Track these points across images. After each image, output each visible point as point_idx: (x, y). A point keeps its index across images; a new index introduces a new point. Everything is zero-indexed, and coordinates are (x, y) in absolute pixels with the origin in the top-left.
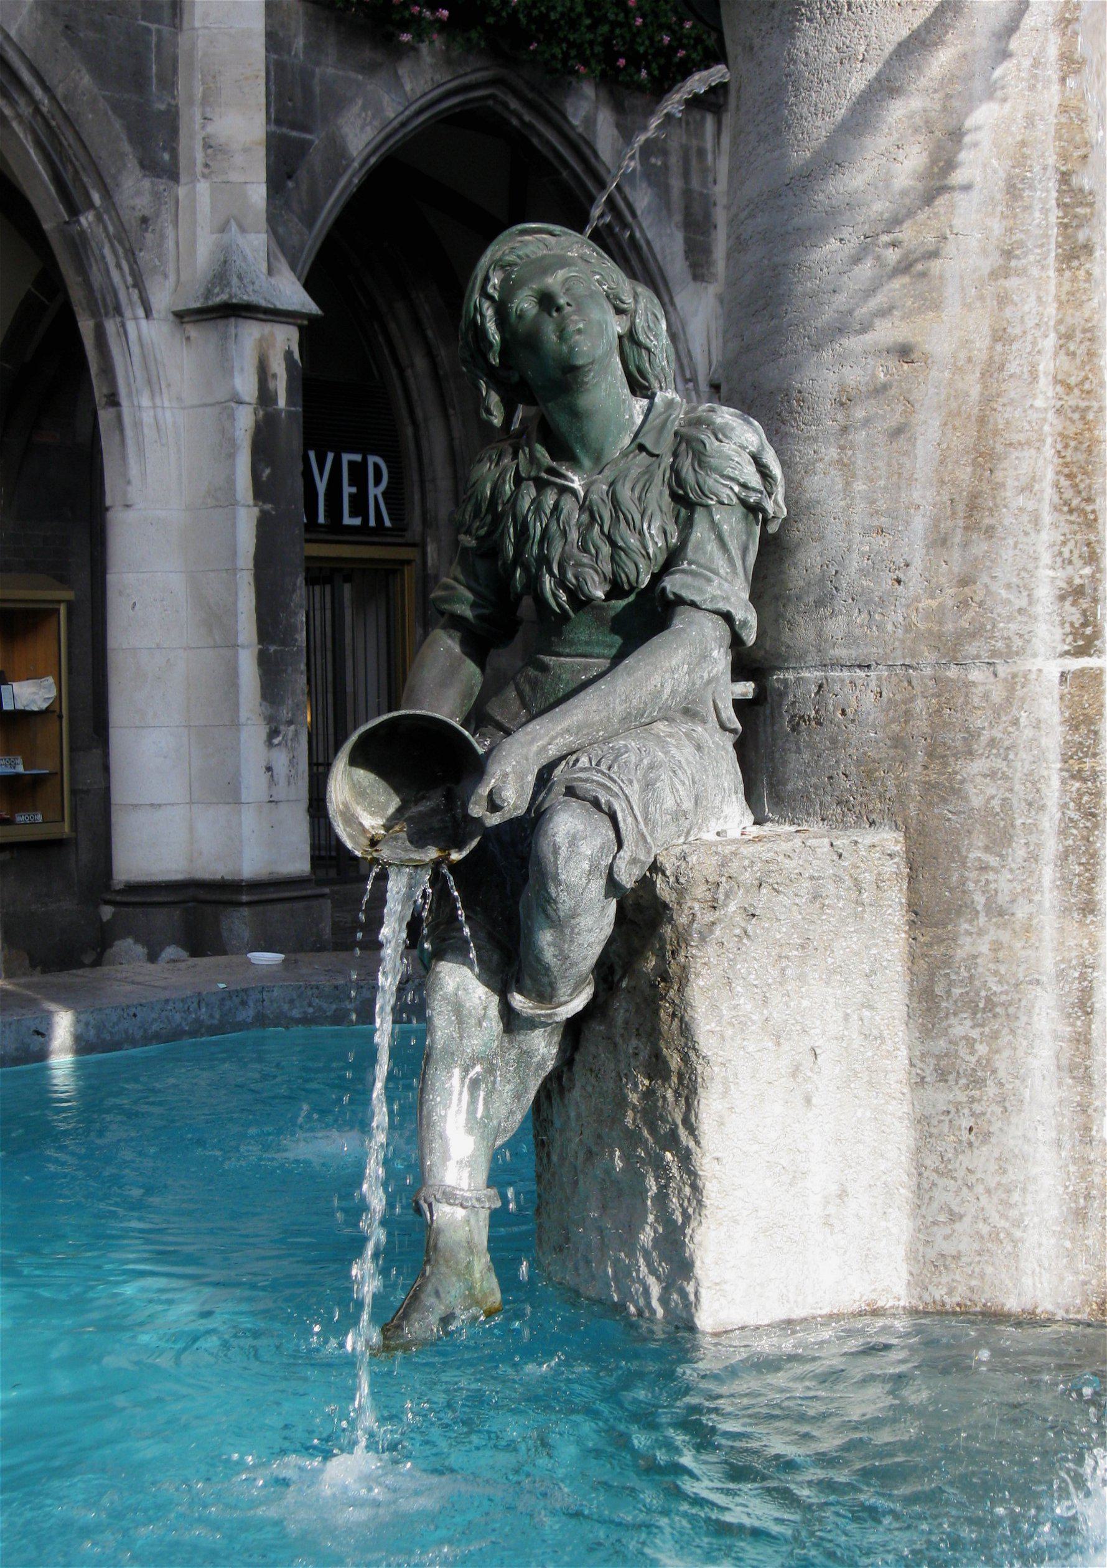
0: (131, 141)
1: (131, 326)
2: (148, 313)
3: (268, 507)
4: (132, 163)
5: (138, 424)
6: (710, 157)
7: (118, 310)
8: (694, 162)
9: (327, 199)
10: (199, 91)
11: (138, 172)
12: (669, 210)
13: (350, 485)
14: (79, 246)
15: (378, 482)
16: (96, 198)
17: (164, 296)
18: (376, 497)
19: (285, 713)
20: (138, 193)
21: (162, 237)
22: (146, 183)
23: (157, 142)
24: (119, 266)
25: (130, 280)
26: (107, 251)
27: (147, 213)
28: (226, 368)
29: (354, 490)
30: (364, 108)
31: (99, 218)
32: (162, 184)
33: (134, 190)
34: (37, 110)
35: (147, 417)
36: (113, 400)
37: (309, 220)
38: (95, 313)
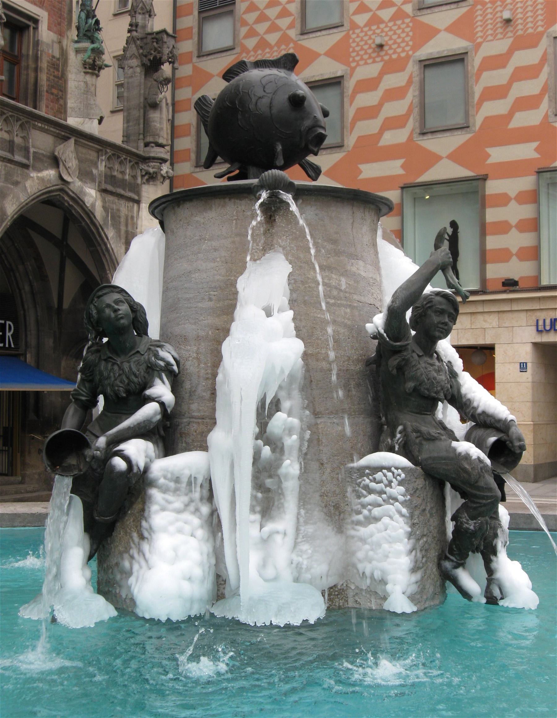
6: (135, 219)
8: (130, 221)
12: (120, 236)
30: (13, 198)
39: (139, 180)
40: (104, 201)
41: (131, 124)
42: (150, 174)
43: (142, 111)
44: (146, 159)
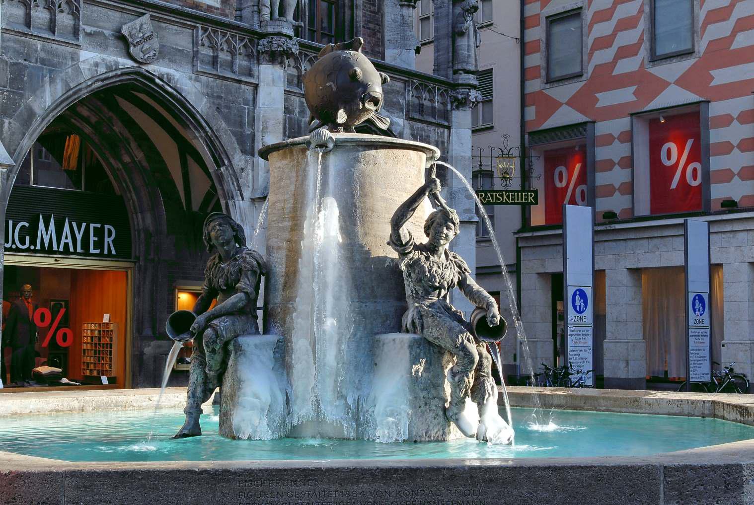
0: (238, 144)
2: (243, 199)
4: (238, 151)
6: (446, 144)
7: (233, 198)
10: (261, 127)
13: (94, 236)
14: (220, 177)
15: (110, 236)
16: (226, 162)
18: (108, 242)
20: (240, 161)
21: (248, 174)
22: (243, 157)
24: (233, 184)
25: (237, 188)
29: (96, 239)
31: (227, 169)
32: (248, 157)
34: (207, 135)
38: (225, 198)
39: (449, 107)
40: (412, 128)
41: (440, 53)
42: (459, 100)
43: (450, 40)
44: (455, 86)
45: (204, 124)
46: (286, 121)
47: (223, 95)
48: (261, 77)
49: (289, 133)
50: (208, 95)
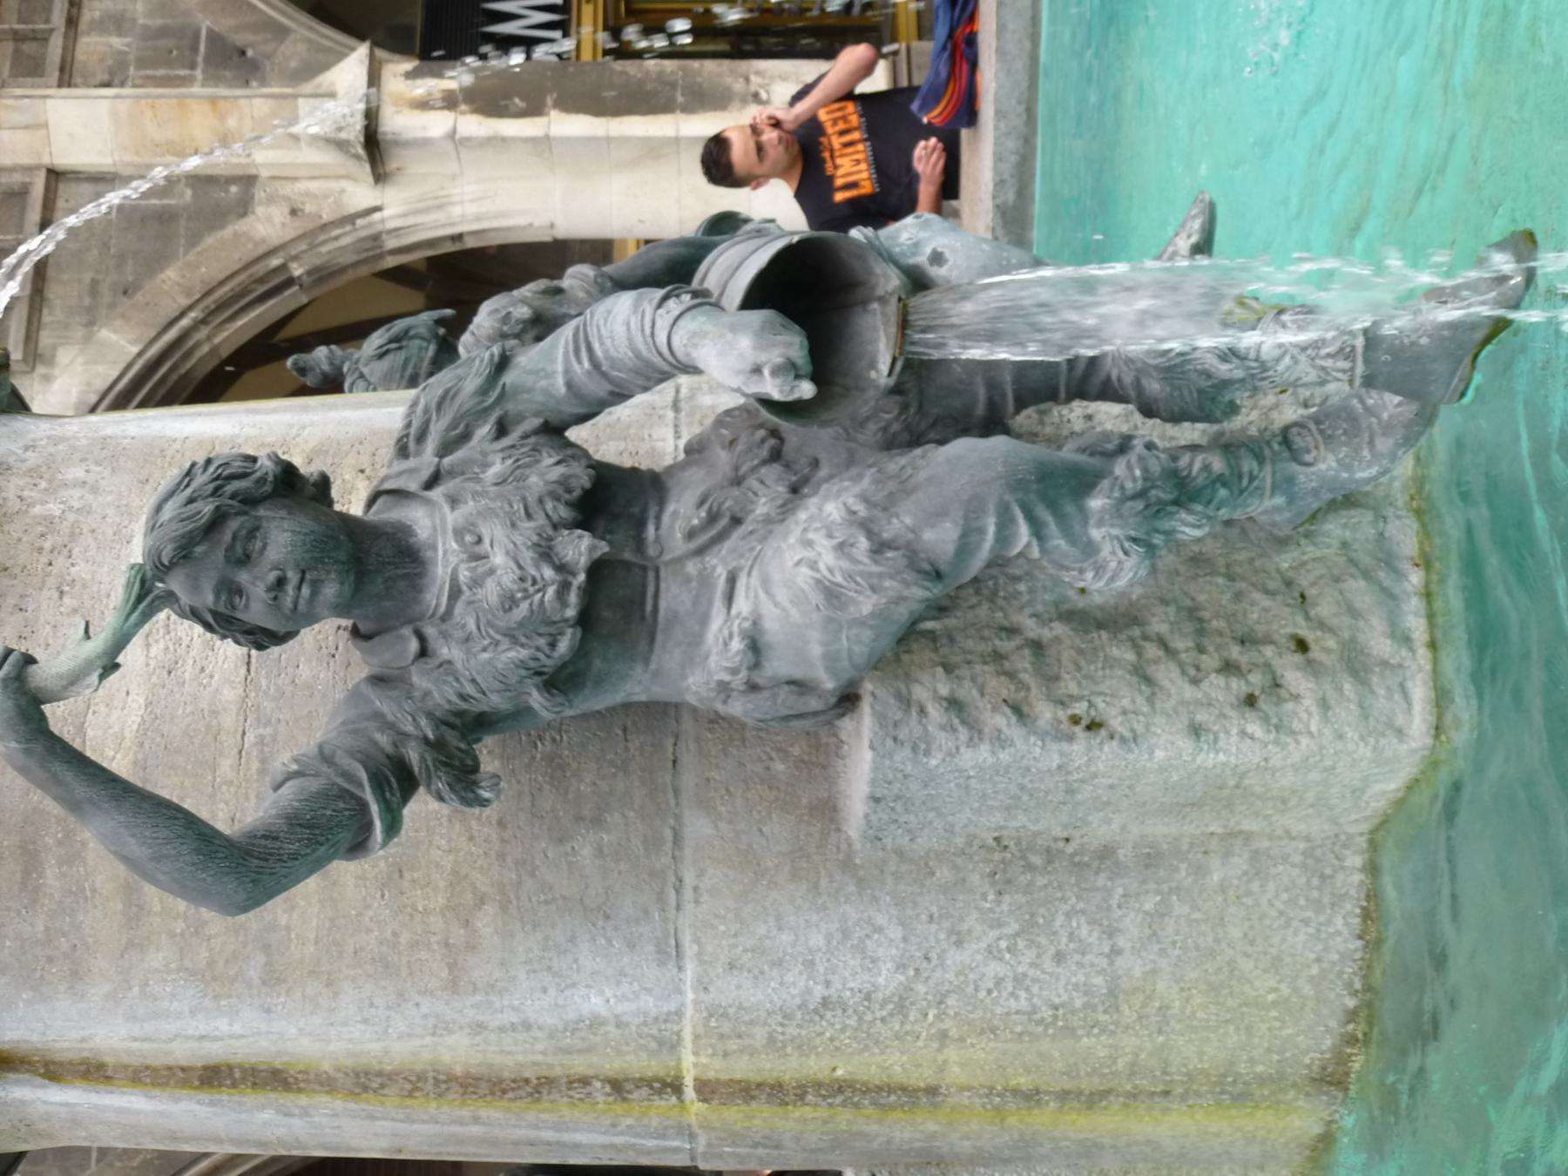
0: (222, 227)
1: (390, 225)
2: (378, 209)
3: (549, 101)
4: (242, 226)
5: (478, 218)
7: (376, 238)
9: (261, 11)
11: (250, 219)
14: (321, 275)
16: (275, 262)
17: (359, 193)
19: (738, 86)
20: (269, 219)
21: (308, 194)
22: (260, 210)
23: (222, 196)
24: (336, 238)
25: (348, 228)
26: (324, 249)
27: (287, 210)
28: (424, 143)
31: (295, 258)
32: (259, 194)
33: (267, 225)
34: (203, 322)
35: (471, 209)
36: (458, 238)
37: (281, 32)
38: (381, 256)
45: (172, 334)
46: (148, 77)
47: (88, 277)
48: (26, 160)
49: (183, 67)
50: (90, 324)
